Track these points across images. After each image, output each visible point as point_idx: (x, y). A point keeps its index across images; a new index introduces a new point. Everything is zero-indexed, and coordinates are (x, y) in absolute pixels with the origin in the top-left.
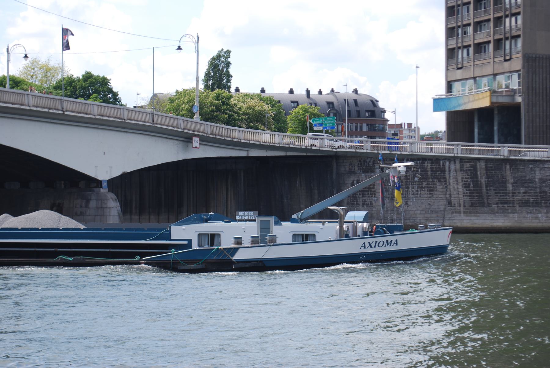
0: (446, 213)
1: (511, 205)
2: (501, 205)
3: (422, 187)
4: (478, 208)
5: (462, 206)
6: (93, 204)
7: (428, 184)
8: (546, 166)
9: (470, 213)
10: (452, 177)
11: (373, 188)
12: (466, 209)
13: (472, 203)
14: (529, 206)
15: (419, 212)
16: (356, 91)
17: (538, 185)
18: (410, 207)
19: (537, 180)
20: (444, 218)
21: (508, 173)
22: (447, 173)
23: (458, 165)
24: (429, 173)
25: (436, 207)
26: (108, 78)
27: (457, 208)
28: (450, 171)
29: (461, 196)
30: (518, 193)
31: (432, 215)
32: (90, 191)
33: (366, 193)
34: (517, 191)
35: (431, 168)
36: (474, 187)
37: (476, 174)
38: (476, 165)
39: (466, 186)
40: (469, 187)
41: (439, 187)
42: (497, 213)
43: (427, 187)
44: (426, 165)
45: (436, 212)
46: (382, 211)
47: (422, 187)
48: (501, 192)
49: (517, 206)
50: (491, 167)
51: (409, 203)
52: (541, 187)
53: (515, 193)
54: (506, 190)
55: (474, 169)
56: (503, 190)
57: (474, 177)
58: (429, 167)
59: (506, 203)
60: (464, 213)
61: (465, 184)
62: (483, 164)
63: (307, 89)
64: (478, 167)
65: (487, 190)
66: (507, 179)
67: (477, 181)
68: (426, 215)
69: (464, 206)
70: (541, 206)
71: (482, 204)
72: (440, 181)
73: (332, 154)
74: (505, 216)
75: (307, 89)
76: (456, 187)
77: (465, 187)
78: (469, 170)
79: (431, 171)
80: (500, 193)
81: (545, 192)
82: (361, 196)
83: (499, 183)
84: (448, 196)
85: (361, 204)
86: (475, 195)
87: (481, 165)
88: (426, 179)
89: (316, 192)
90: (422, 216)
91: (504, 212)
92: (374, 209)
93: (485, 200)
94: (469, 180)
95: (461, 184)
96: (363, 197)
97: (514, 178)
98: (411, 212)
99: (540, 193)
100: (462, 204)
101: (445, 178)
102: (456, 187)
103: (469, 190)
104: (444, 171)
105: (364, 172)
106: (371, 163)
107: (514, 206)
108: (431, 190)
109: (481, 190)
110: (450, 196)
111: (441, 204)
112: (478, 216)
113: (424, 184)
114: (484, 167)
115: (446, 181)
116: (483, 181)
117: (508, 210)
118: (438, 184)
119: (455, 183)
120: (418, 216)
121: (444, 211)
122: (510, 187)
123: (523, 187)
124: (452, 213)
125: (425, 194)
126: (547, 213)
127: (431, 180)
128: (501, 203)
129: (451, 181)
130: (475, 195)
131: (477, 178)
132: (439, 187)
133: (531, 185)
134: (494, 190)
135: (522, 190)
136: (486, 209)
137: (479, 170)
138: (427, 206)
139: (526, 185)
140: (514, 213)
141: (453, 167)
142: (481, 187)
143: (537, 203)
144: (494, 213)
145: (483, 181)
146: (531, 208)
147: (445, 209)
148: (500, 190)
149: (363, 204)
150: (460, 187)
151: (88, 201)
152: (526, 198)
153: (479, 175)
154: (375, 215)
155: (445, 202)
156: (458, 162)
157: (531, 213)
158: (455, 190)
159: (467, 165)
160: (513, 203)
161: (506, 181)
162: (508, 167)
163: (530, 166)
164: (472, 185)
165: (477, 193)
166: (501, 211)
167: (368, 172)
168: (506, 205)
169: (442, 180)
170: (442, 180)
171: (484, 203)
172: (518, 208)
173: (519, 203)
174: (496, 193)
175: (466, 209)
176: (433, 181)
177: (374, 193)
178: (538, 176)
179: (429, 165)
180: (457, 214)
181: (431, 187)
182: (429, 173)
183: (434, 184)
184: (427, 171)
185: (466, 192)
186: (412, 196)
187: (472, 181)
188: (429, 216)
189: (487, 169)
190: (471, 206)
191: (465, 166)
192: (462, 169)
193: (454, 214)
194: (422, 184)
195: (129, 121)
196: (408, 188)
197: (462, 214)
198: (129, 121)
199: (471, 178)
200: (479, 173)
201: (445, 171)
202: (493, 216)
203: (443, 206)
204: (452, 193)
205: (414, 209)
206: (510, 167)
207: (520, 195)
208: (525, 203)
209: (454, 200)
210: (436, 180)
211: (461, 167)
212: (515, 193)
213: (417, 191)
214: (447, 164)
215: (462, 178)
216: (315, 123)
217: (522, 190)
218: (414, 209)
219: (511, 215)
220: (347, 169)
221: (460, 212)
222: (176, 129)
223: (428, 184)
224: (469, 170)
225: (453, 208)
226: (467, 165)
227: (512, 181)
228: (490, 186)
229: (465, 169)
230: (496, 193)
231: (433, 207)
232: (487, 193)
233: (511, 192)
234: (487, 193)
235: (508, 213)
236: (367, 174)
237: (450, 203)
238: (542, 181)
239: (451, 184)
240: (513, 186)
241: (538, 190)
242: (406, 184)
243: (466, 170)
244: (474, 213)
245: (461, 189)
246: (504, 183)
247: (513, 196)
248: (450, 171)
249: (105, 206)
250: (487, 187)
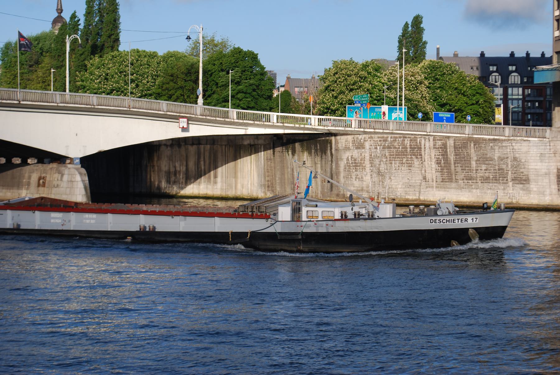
0: (422, 187)
1: (475, 181)
2: (466, 181)
3: (402, 163)
4: (447, 183)
5: (435, 181)
6: (65, 178)
7: (407, 160)
8: (504, 144)
9: (441, 188)
10: (426, 154)
11: (364, 163)
12: (438, 184)
13: (443, 179)
14: (489, 183)
15: (400, 186)
17: (497, 163)
18: (393, 181)
19: (496, 158)
20: (420, 192)
21: (473, 150)
22: (423, 150)
23: (432, 143)
24: (409, 150)
25: (414, 181)
26: (255, 53)
27: (430, 183)
28: (425, 148)
29: (434, 172)
30: (481, 170)
31: (410, 190)
32: (65, 167)
33: (358, 168)
34: (479, 168)
35: (410, 145)
36: (444, 163)
37: (446, 152)
38: (446, 143)
39: (438, 163)
40: (440, 163)
41: (416, 163)
42: (463, 188)
43: (407, 163)
44: (406, 142)
45: (414, 187)
46: (370, 185)
47: (402, 163)
48: (467, 168)
49: (480, 182)
50: (459, 145)
51: (392, 178)
52: (499, 164)
53: (478, 170)
54: (471, 167)
56: (468, 167)
57: (445, 154)
58: (408, 144)
59: (471, 179)
60: (436, 187)
61: (437, 160)
63: (527, 52)
64: (448, 145)
65: (455, 167)
66: (472, 156)
67: (447, 158)
68: (405, 189)
69: (436, 182)
70: (500, 183)
71: (451, 180)
72: (417, 158)
73: (326, 132)
74: (470, 191)
75: (527, 52)
76: (430, 163)
77: (437, 163)
78: (441, 148)
79: (410, 148)
80: (465, 170)
81: (502, 169)
82: (354, 170)
83: (465, 160)
84: (423, 172)
85: (354, 177)
86: (445, 171)
88: (406, 155)
89: (319, 166)
90: (403, 190)
91: (469, 187)
92: (364, 183)
93: (454, 176)
94: (440, 157)
95: (434, 160)
96: (356, 171)
97: (477, 155)
98: (393, 186)
99: (499, 170)
100: (435, 179)
101: (421, 155)
102: (430, 163)
103: (441, 166)
104: (420, 148)
105: (356, 148)
106: (362, 141)
107: (476, 182)
108: (410, 166)
109: (450, 166)
110: (425, 172)
111: (418, 178)
112: (448, 191)
113: (405, 160)
114: (453, 145)
115: (421, 158)
116: (452, 157)
117: (472, 185)
118: (415, 160)
119: (429, 159)
120: (399, 190)
121: (420, 186)
122: (474, 164)
123: (485, 164)
124: (427, 187)
125: (405, 168)
126: (504, 189)
127: (410, 157)
128: (467, 179)
129: (426, 158)
130: (445, 171)
131: (447, 155)
132: (416, 163)
133: (491, 162)
134: (461, 167)
135: (484, 167)
136: (453, 185)
137: (448, 148)
138: (407, 181)
139: (487, 162)
140: (477, 189)
142: (450, 164)
143: (496, 180)
144: (460, 188)
145: (452, 157)
146: (491, 184)
147: (421, 184)
148: (465, 167)
149: (356, 178)
150: (433, 163)
151: (62, 175)
152: (487, 175)
153: (449, 153)
154: (365, 188)
155: (421, 177)
157: (491, 189)
158: (429, 166)
160: (476, 180)
161: (470, 158)
162: (472, 145)
163: (491, 145)
164: (443, 162)
165: (446, 169)
166: (467, 187)
167: (359, 148)
168: (470, 181)
169: (419, 157)
170: (419, 157)
171: (452, 179)
172: (480, 184)
173: (481, 180)
174: (462, 169)
175: (438, 184)
176: (411, 158)
177: (364, 168)
178: (497, 155)
179: (408, 142)
180: (430, 189)
181: (410, 163)
182: (409, 150)
183: (412, 160)
184: (407, 148)
185: (438, 168)
186: (395, 171)
187: (443, 158)
188: (408, 190)
189: (455, 147)
190: (442, 182)
191: (437, 144)
193: (428, 189)
194: (402, 160)
195: (100, 107)
196: (391, 163)
197: (435, 189)
198: (100, 107)
199: (442, 155)
200: (448, 150)
201: (421, 148)
202: (459, 191)
203: (419, 181)
204: (427, 169)
205: (396, 184)
206: (474, 145)
207: (482, 171)
208: (486, 180)
209: (429, 176)
210: (414, 157)
211: (434, 145)
212: (478, 170)
213: (399, 166)
215: (435, 155)
216: (356, 99)
217: (484, 167)
218: (396, 184)
219: (474, 191)
220: (344, 146)
221: (433, 187)
222: (156, 112)
223: (407, 160)
224: (441, 148)
225: (427, 183)
226: (439, 143)
227: (475, 158)
228: (458, 163)
229: (437, 147)
230: (462, 169)
231: (411, 181)
232: (455, 170)
233: (474, 169)
234: (455, 170)
235: (472, 188)
236: (359, 150)
237: (425, 178)
238: (501, 159)
239: (426, 160)
240: (477, 163)
241: (497, 167)
242: (390, 160)
243: (438, 148)
244: (444, 188)
245: (434, 166)
246: (468, 159)
247: (476, 172)
248: (425, 148)
249: (73, 180)
250: (455, 163)
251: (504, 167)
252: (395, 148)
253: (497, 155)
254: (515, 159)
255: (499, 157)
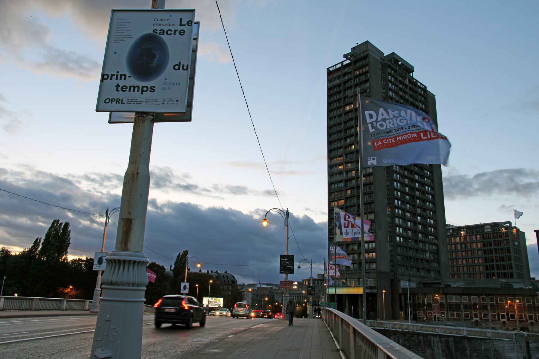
16: (226, 272)
21: (467, 345)
22: (432, 343)
23: (438, 339)
39: (443, 351)
55: (447, 341)
62: (452, 339)
72: (428, 348)
81: (488, 356)
87: (451, 340)
113: (420, 349)
116: (453, 349)
118: (427, 349)
122: (468, 352)
131: (449, 346)
132: (428, 351)
135: (475, 355)
141: (435, 340)
145: (453, 349)
150: (440, 351)
156: (438, 337)
159: (444, 339)
162: (466, 341)
192: (440, 341)
214: (432, 338)
217: (475, 355)
226: (444, 339)
238: (486, 350)
250: (455, 352)
251: (489, 355)
252: (412, 341)
253: (483, 348)
254: (495, 350)
255: (485, 349)
